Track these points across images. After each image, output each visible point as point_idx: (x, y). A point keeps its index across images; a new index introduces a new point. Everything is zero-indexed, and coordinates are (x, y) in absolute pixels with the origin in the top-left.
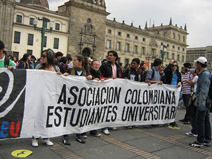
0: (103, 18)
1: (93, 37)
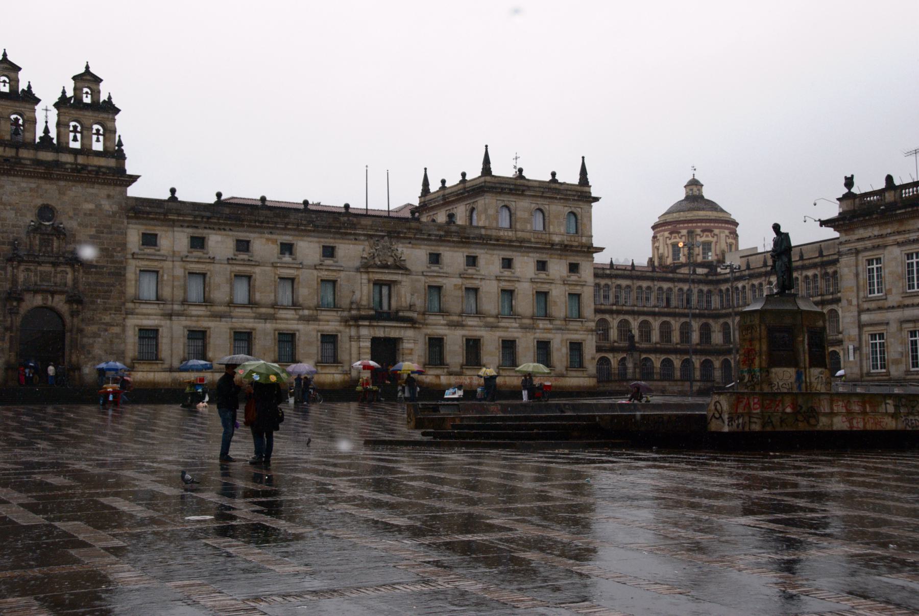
0: (109, 196)
1: (69, 270)
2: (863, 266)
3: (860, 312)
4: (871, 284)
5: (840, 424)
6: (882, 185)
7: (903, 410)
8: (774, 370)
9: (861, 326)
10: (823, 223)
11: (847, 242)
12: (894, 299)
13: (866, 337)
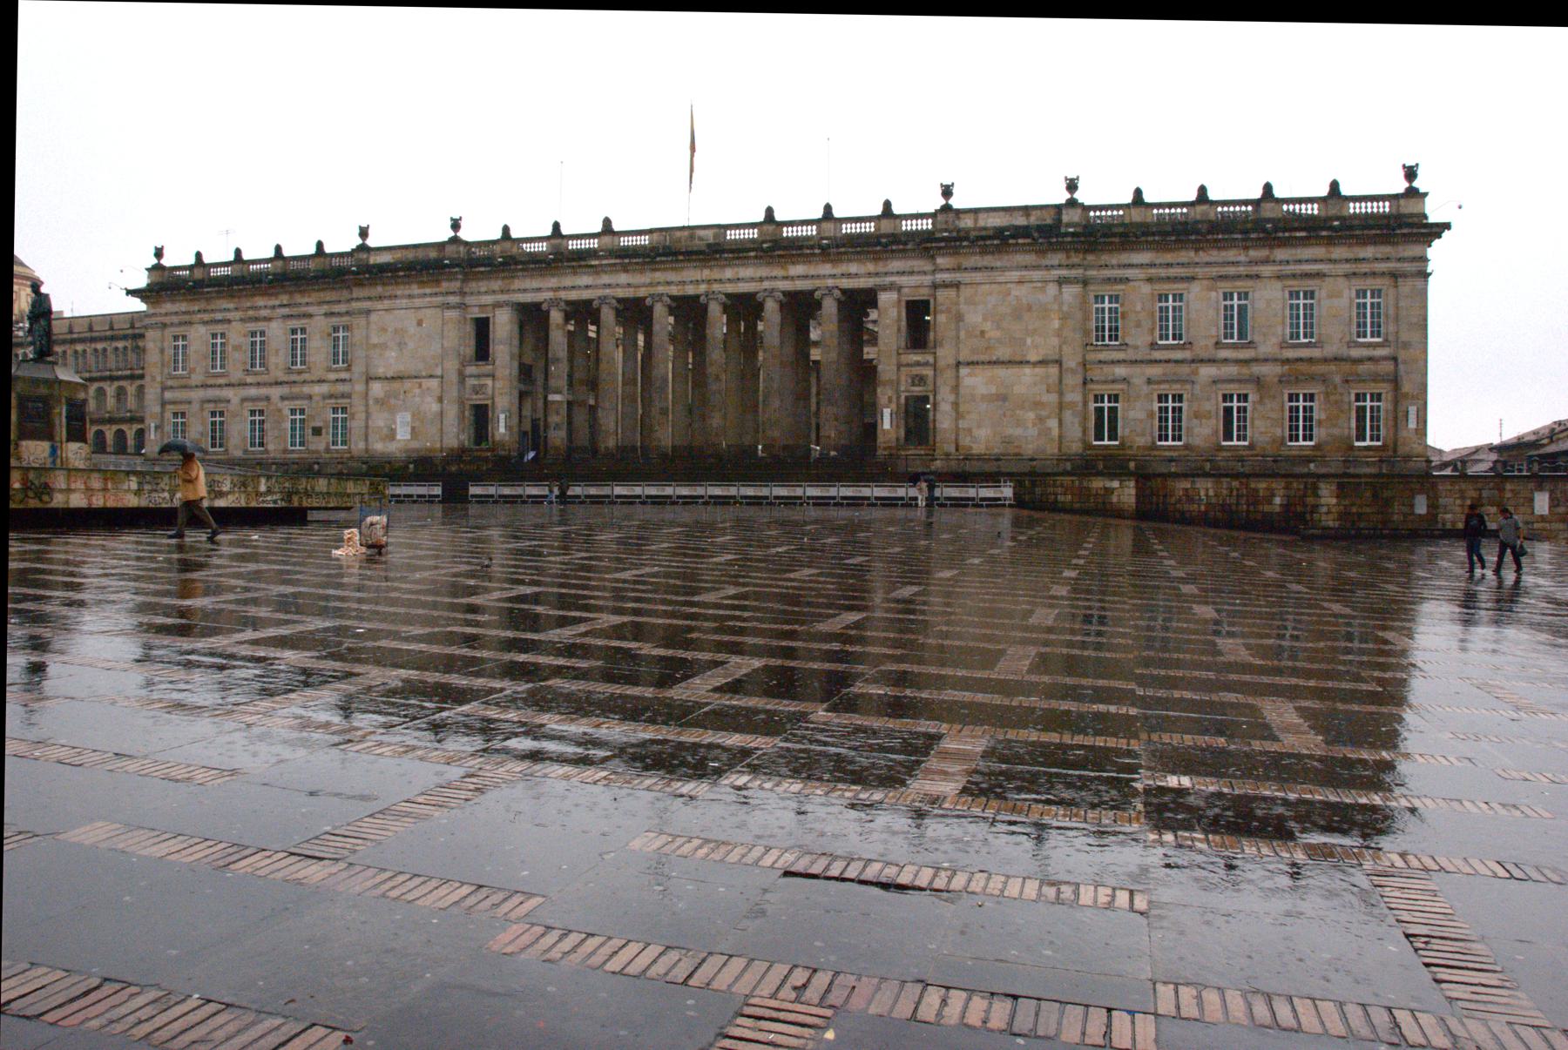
2: (169, 343)
3: (164, 389)
4: (176, 361)
5: (77, 501)
6: (192, 261)
7: (147, 487)
8: (24, 443)
9: (164, 404)
10: (130, 292)
11: (154, 315)
12: (197, 378)
13: (168, 415)
